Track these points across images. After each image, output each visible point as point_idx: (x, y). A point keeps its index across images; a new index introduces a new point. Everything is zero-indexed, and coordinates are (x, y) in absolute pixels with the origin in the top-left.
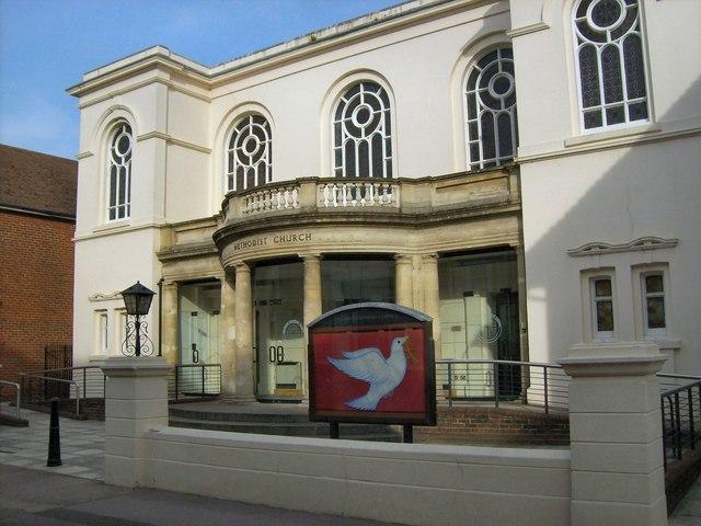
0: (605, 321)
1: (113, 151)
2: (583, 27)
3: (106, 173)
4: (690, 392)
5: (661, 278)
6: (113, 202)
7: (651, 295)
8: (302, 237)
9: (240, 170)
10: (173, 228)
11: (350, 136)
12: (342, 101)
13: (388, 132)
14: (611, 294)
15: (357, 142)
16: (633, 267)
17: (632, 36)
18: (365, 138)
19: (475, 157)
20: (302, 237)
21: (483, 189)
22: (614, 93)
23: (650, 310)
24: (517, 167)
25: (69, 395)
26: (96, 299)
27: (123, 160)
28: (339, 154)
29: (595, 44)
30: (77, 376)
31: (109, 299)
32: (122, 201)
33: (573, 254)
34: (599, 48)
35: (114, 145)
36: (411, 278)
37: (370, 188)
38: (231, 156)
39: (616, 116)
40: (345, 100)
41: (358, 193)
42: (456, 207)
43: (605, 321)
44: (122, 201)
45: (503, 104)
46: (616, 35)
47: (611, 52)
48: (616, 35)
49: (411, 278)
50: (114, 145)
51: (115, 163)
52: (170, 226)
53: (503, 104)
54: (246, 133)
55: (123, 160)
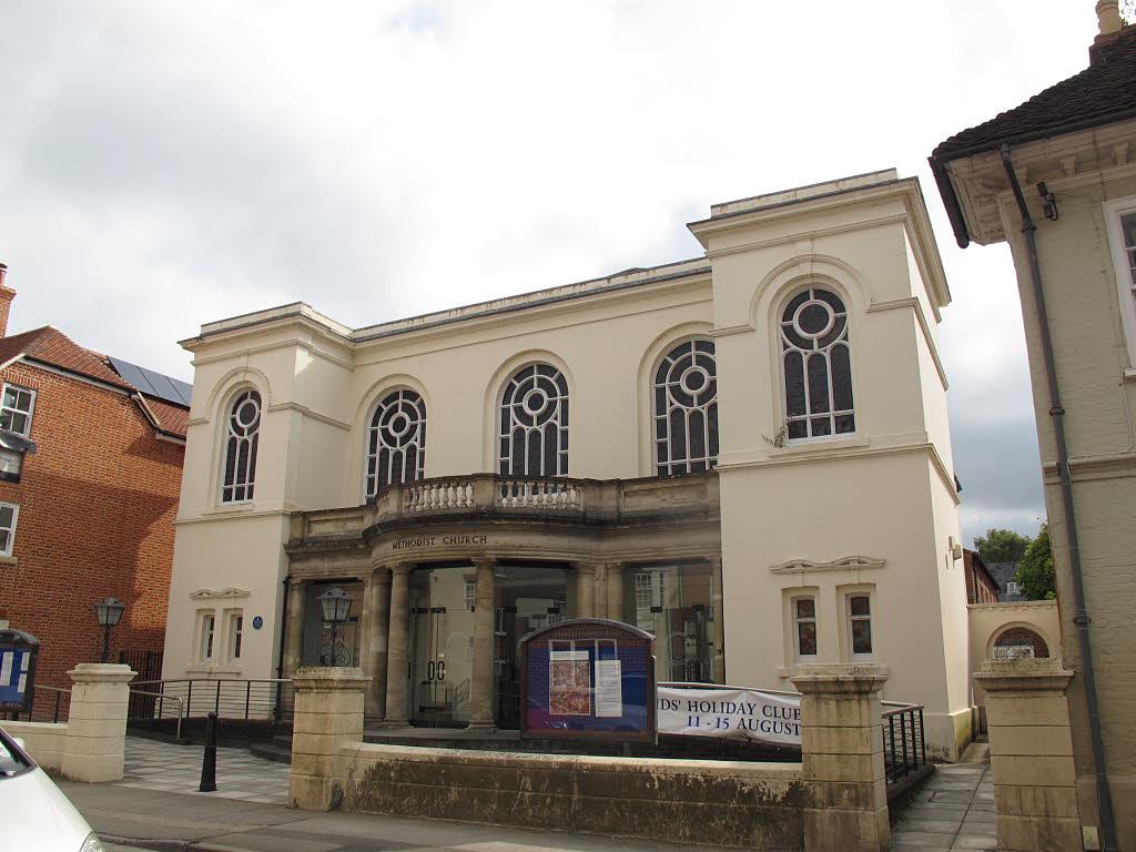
0: (808, 644)
1: (234, 420)
2: (789, 331)
3: (222, 446)
4: (891, 720)
5: (867, 600)
6: (229, 480)
7: (857, 618)
8: (476, 539)
9: (385, 452)
10: (303, 518)
11: (519, 424)
12: (511, 383)
13: (565, 422)
14: (869, 614)
15: (528, 430)
16: (837, 587)
17: (838, 346)
18: (537, 427)
19: (662, 456)
20: (476, 539)
21: (677, 497)
22: (819, 403)
23: (856, 633)
24: (716, 475)
25: (623, 664)
26: (200, 596)
27: (246, 432)
28: (372, 461)
29: (802, 351)
30: (169, 690)
31: (218, 597)
32: (241, 479)
33: (776, 571)
34: (805, 355)
35: (234, 412)
36: (594, 589)
37: (527, 487)
38: (374, 434)
39: (821, 428)
40: (515, 382)
41: (510, 491)
42: (647, 514)
43: (808, 644)
44: (241, 479)
45: (695, 401)
46: (823, 342)
47: (817, 361)
48: (823, 342)
49: (594, 589)
50: (234, 412)
51: (234, 434)
52: (305, 515)
53: (695, 401)
54: (395, 409)
55: (246, 432)
